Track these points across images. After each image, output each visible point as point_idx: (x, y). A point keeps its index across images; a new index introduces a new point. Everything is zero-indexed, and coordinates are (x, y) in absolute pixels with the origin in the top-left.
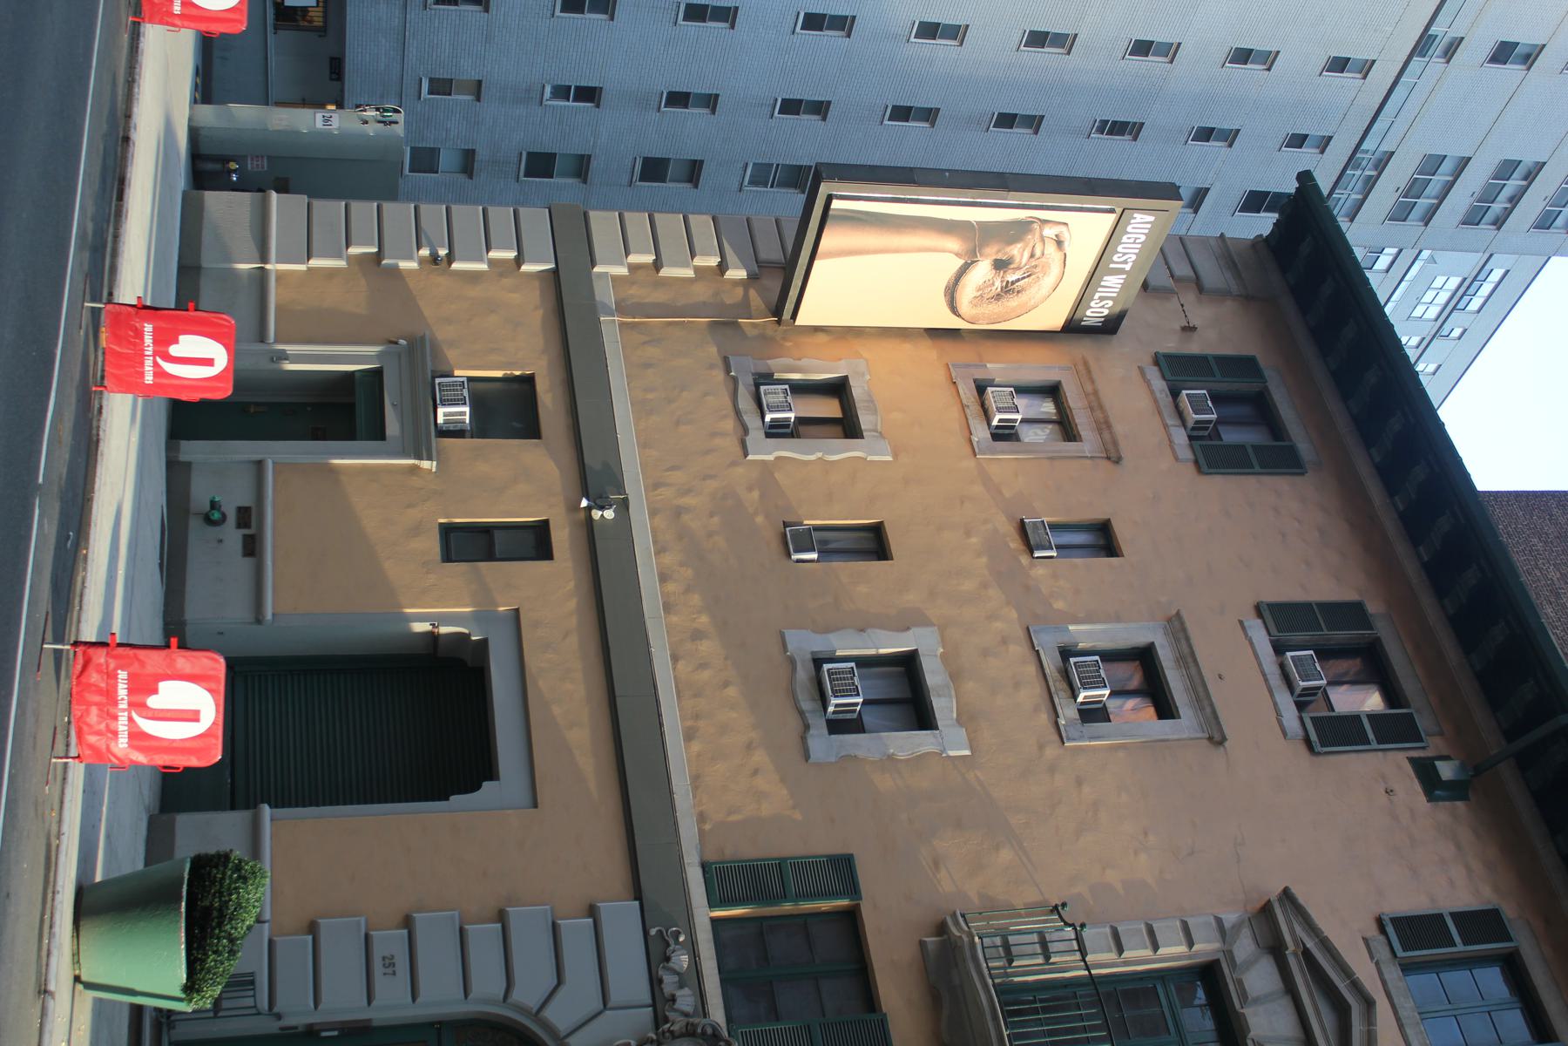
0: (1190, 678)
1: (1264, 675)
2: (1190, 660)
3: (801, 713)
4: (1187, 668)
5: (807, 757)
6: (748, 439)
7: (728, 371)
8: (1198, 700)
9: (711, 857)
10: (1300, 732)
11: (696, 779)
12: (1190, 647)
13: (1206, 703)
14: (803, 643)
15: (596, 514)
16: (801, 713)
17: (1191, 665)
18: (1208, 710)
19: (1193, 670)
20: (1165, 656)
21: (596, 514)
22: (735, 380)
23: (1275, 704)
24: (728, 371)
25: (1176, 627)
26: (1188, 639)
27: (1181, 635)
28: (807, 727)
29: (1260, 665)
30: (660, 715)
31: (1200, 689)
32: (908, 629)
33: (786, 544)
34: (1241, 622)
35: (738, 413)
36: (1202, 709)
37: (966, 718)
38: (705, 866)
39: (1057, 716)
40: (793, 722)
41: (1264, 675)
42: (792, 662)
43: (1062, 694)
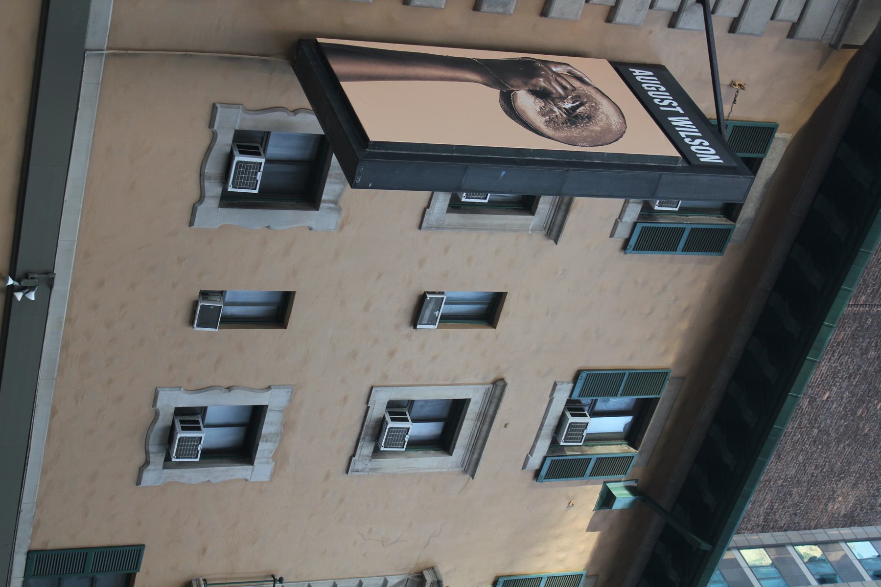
0: (480, 430)
1: (542, 425)
2: (488, 420)
3: (147, 453)
4: (483, 423)
5: (138, 482)
6: (200, 209)
7: (211, 124)
8: (474, 446)
9: (37, 546)
10: (537, 467)
11: (39, 504)
12: (495, 412)
13: (477, 451)
14: (173, 399)
15: (19, 296)
16: (147, 453)
17: (487, 423)
18: (475, 456)
19: (485, 427)
20: (472, 411)
21: (19, 296)
22: (214, 137)
23: (534, 446)
24: (211, 124)
25: (498, 387)
26: (497, 406)
27: (495, 401)
28: (147, 463)
29: (545, 418)
30: (27, 457)
31: (480, 442)
32: (269, 388)
33: (194, 311)
34: (555, 385)
35: (202, 176)
36: (472, 453)
37: (280, 459)
38: (29, 553)
39: (354, 455)
40: (140, 459)
41: (542, 425)
42: (157, 414)
43: (367, 438)
